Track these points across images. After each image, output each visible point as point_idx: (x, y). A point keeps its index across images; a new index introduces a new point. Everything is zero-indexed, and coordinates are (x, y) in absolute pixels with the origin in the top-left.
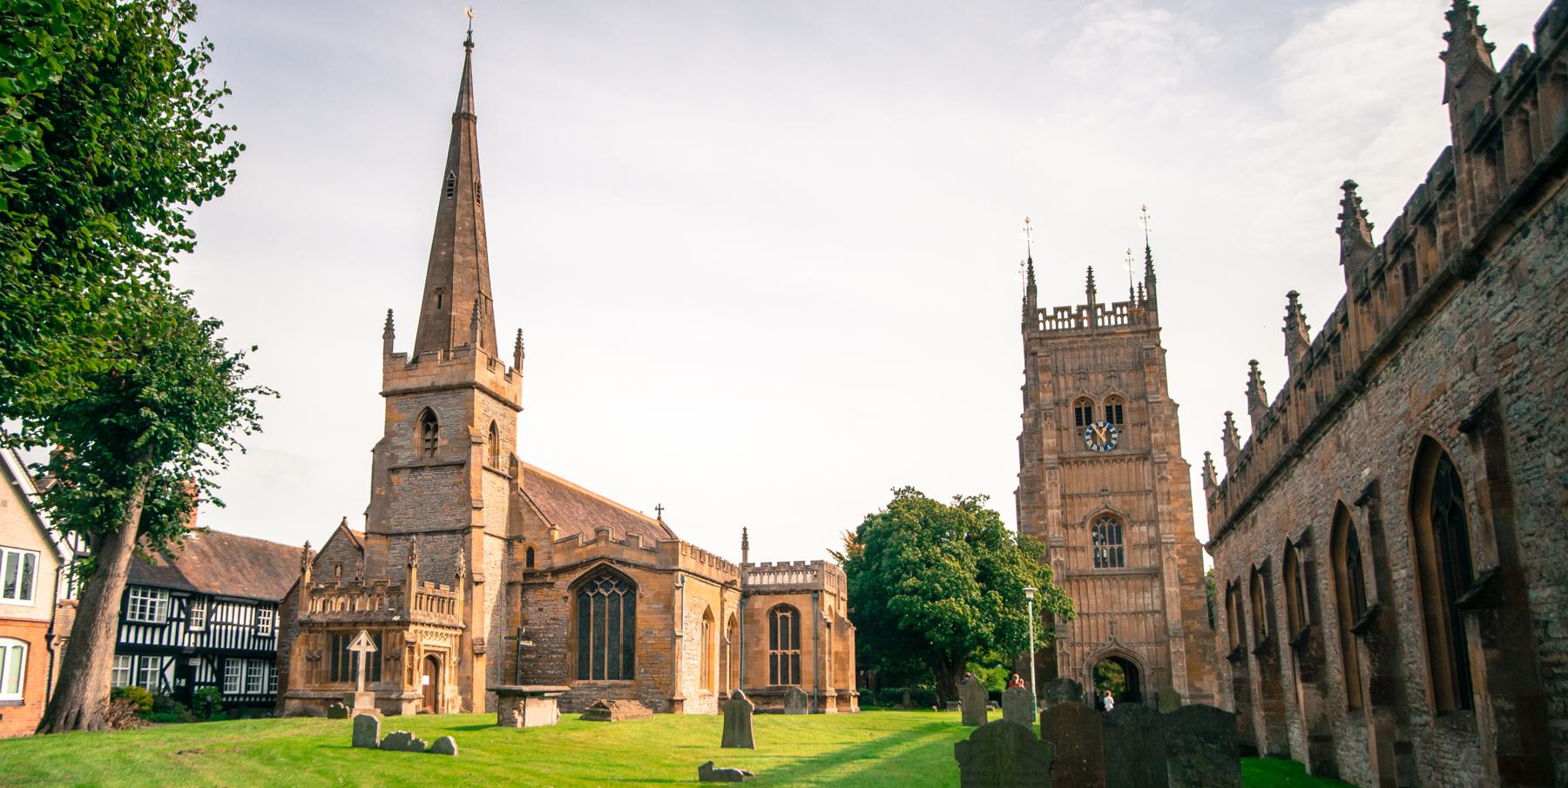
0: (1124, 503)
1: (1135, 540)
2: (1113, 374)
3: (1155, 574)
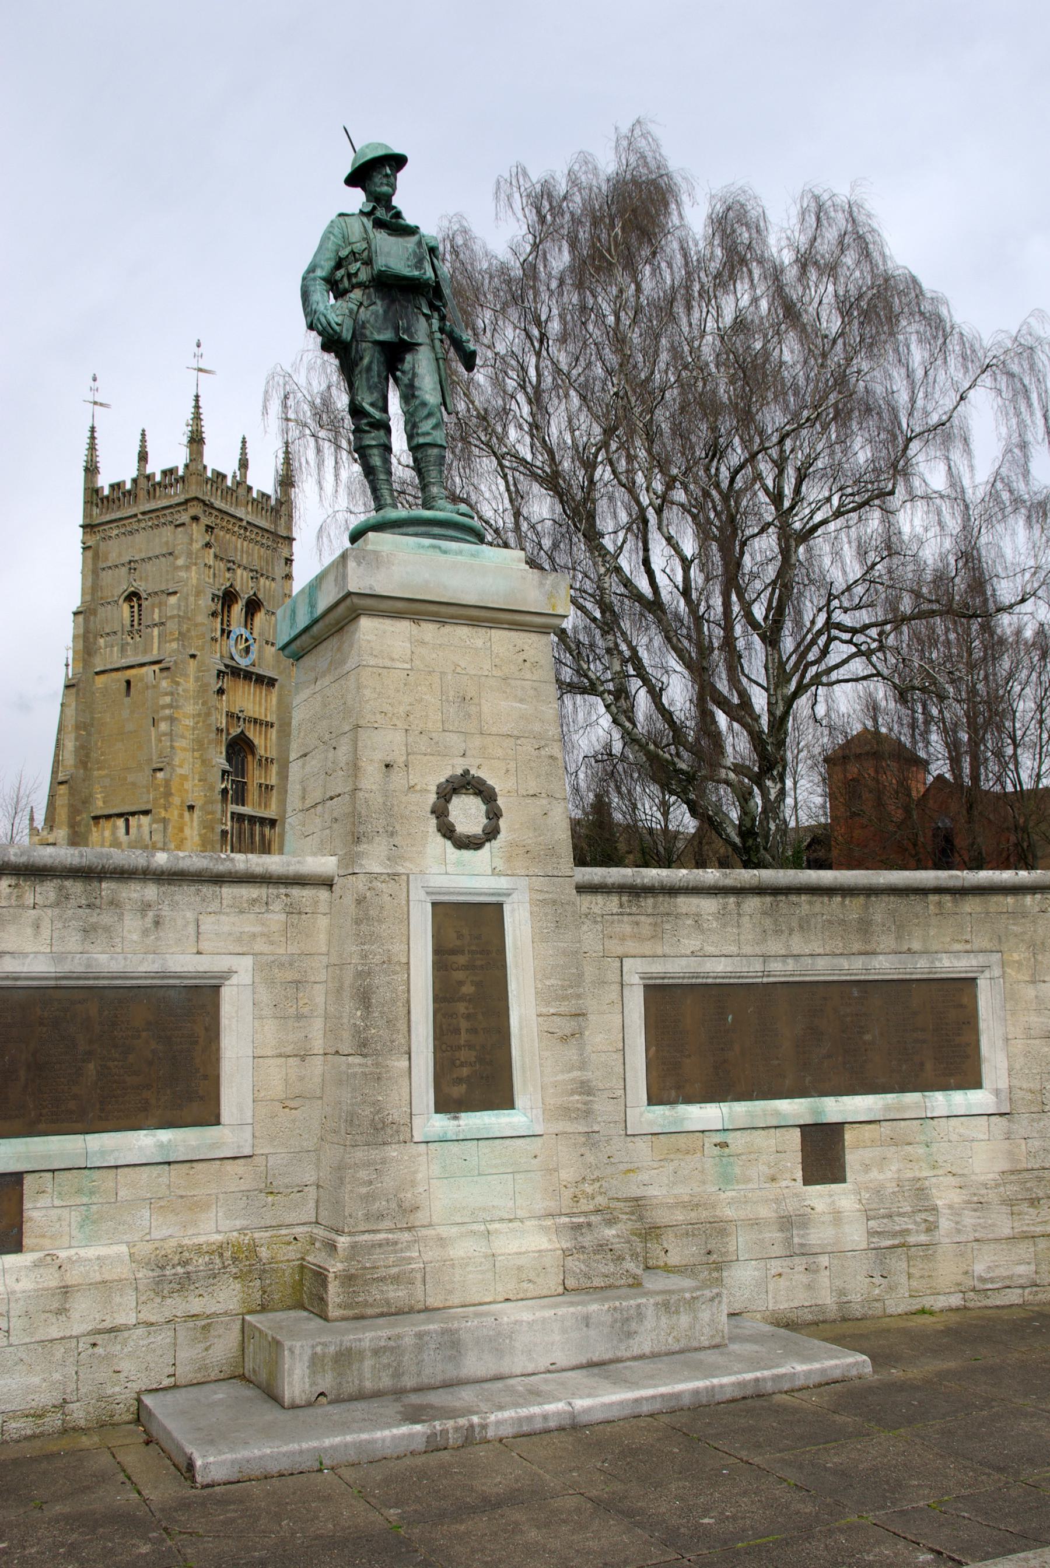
2: (256, 574)
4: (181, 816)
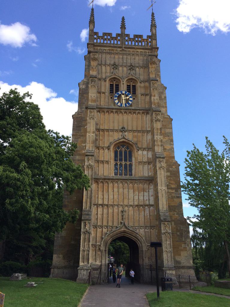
0: (134, 137)
1: (140, 159)
3: (152, 180)
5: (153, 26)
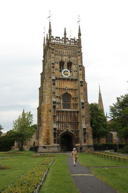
2: (70, 57)
4: (48, 113)
5: (80, 34)
